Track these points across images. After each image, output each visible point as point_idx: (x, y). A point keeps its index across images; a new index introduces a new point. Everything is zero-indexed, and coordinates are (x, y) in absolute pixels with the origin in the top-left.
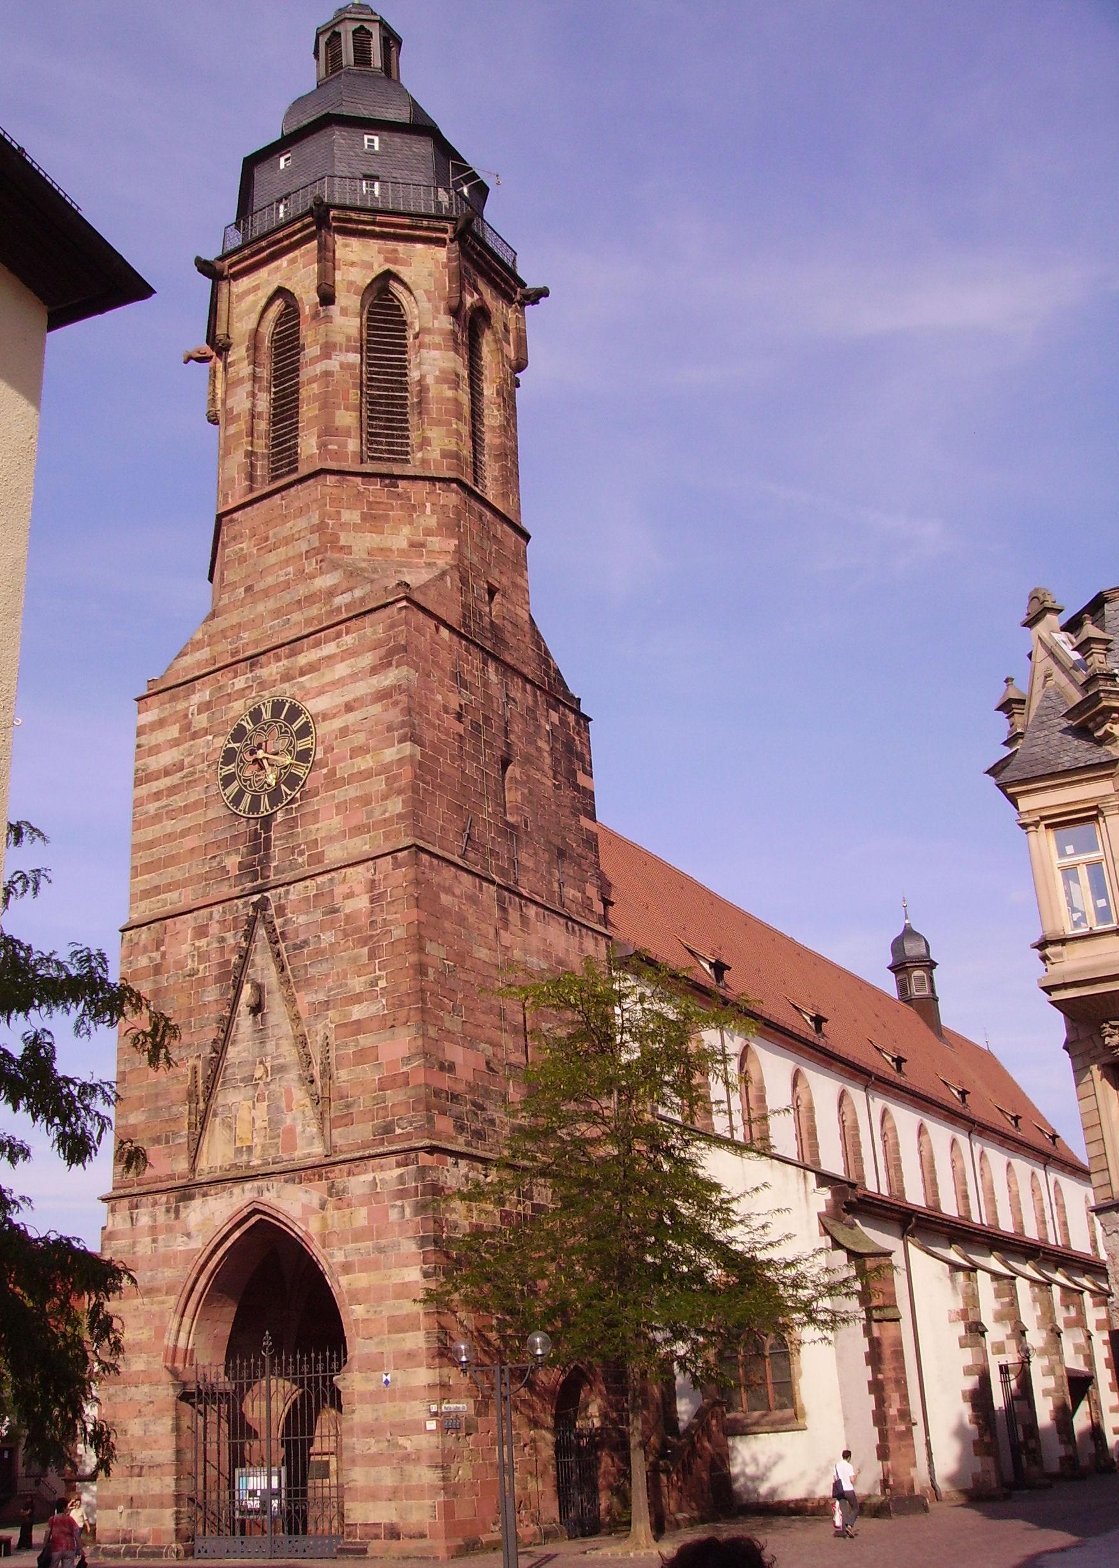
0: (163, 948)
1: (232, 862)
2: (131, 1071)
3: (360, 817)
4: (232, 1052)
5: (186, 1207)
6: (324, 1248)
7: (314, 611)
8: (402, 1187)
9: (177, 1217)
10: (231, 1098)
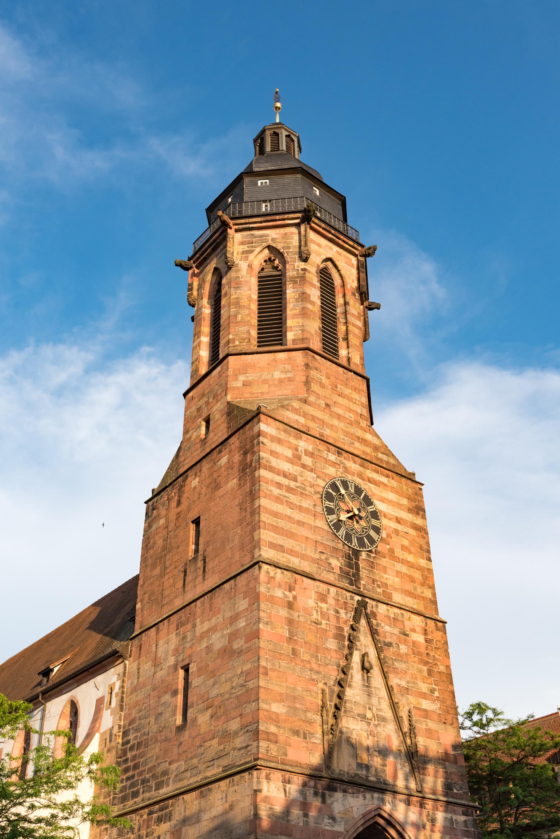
0: (294, 593)
1: (336, 563)
2: (273, 670)
3: (409, 587)
4: (349, 693)
5: (330, 796)
7: (368, 450)
8: (466, 829)
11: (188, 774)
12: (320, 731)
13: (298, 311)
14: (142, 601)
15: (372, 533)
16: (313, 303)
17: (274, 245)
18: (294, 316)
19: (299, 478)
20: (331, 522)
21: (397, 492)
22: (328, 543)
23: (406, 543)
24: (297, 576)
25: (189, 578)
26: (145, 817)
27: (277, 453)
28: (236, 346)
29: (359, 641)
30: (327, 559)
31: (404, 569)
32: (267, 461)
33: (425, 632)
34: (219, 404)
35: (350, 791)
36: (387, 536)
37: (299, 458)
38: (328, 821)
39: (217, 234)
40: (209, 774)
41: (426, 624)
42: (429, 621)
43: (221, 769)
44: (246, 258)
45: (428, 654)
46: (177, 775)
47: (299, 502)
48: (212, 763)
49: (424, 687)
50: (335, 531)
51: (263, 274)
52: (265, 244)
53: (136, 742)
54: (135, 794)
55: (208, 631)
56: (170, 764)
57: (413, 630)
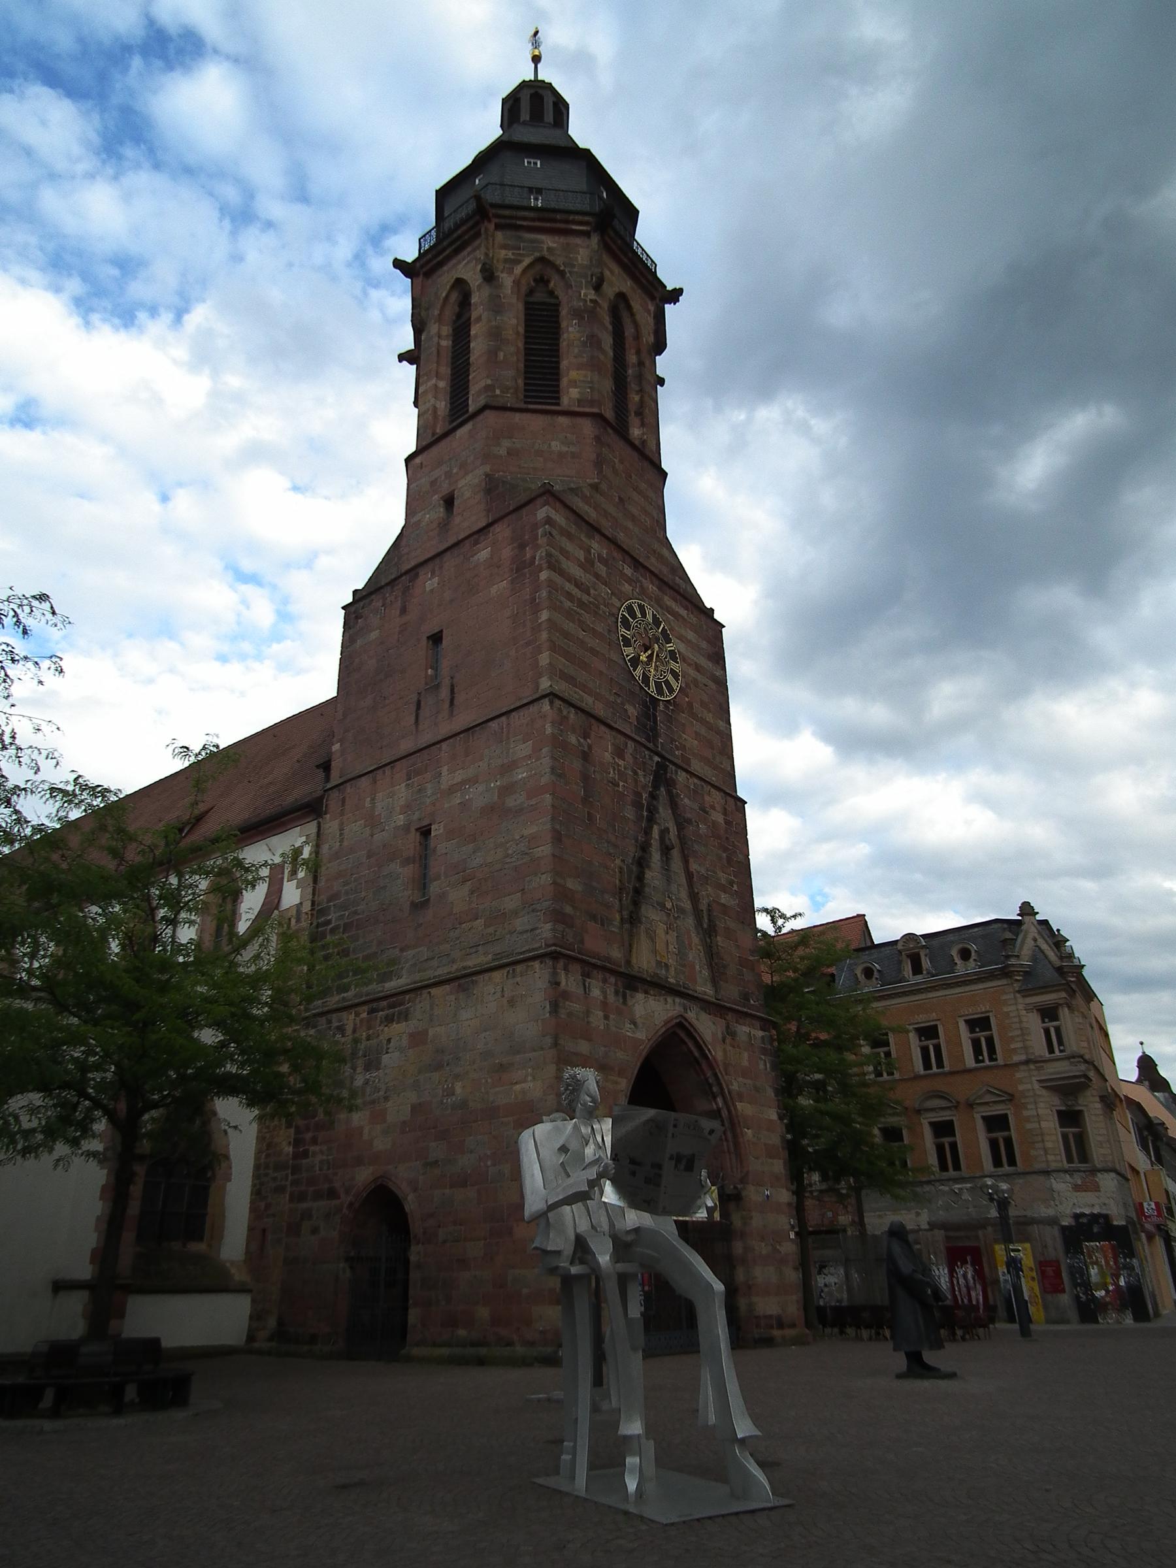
4: (649, 875)
6: (726, 1074)
9: (625, 1002)
10: (651, 914)
11: (435, 963)
12: (618, 916)
13: (585, 360)
14: (341, 741)
15: (670, 678)
16: (604, 352)
17: (551, 258)
18: (579, 367)
19: (592, 591)
20: (627, 656)
21: (696, 632)
22: (624, 684)
23: (706, 698)
24: (593, 721)
25: (425, 712)
26: (364, 1015)
27: (567, 552)
28: (497, 396)
29: (658, 813)
30: (623, 704)
31: (703, 731)
32: (556, 561)
33: (725, 813)
34: (469, 478)
35: (652, 992)
36: (686, 686)
37: (592, 564)
38: (629, 1026)
39: (464, 228)
40: (470, 963)
41: (726, 801)
42: (729, 798)
43: (490, 956)
44: (511, 271)
45: (727, 838)
46: (415, 965)
47: (592, 624)
48: (474, 950)
49: (723, 877)
50: (632, 669)
51: (531, 299)
52: (537, 254)
53: (341, 923)
54: (345, 989)
55: (463, 782)
56: (402, 950)
57: (713, 807)
